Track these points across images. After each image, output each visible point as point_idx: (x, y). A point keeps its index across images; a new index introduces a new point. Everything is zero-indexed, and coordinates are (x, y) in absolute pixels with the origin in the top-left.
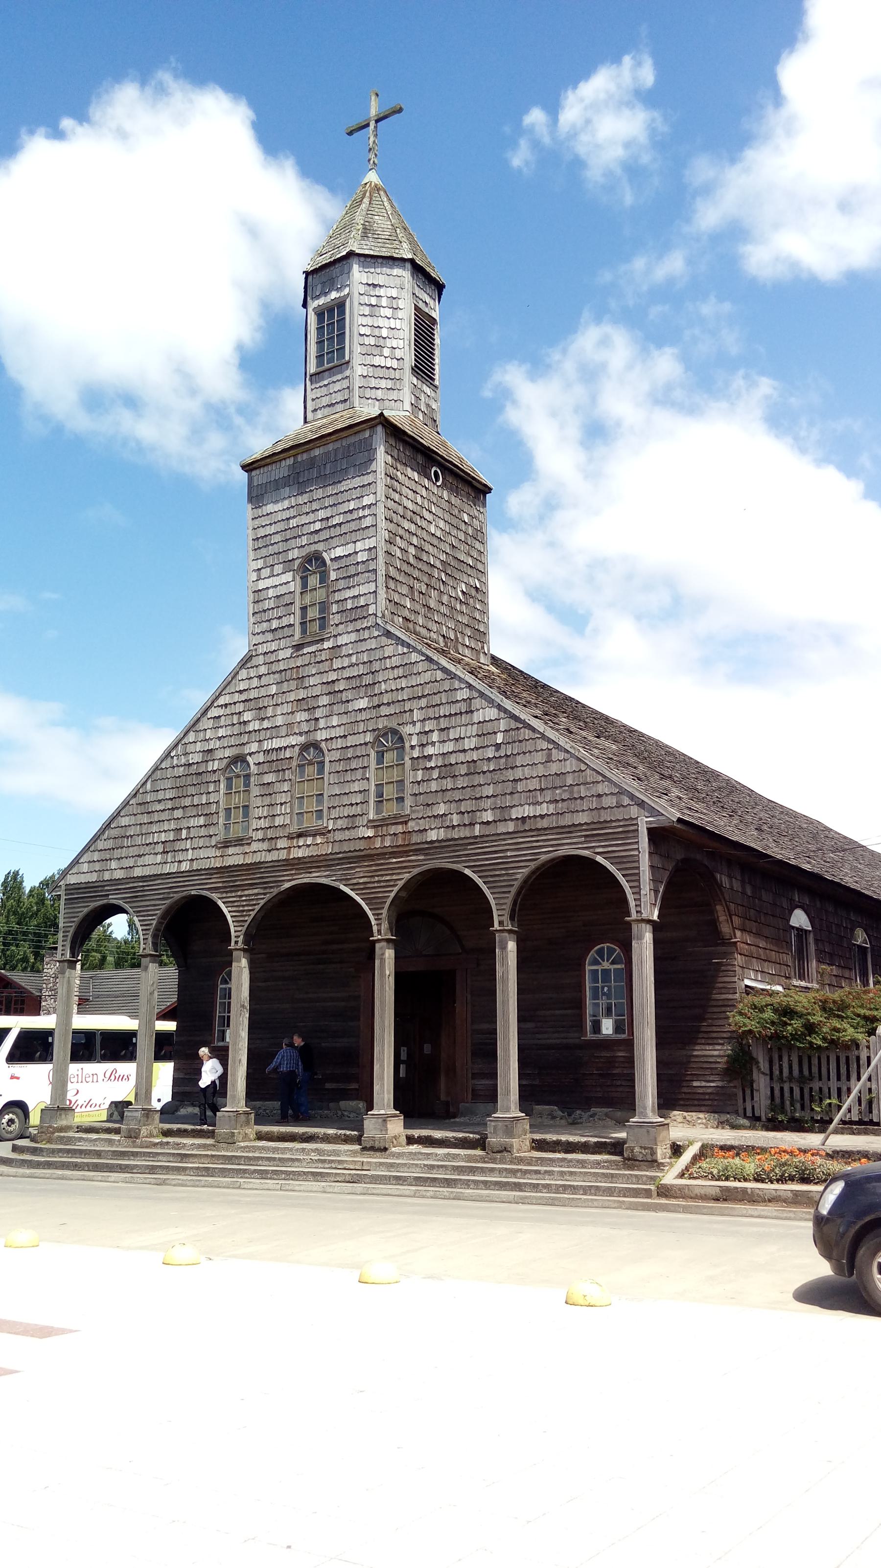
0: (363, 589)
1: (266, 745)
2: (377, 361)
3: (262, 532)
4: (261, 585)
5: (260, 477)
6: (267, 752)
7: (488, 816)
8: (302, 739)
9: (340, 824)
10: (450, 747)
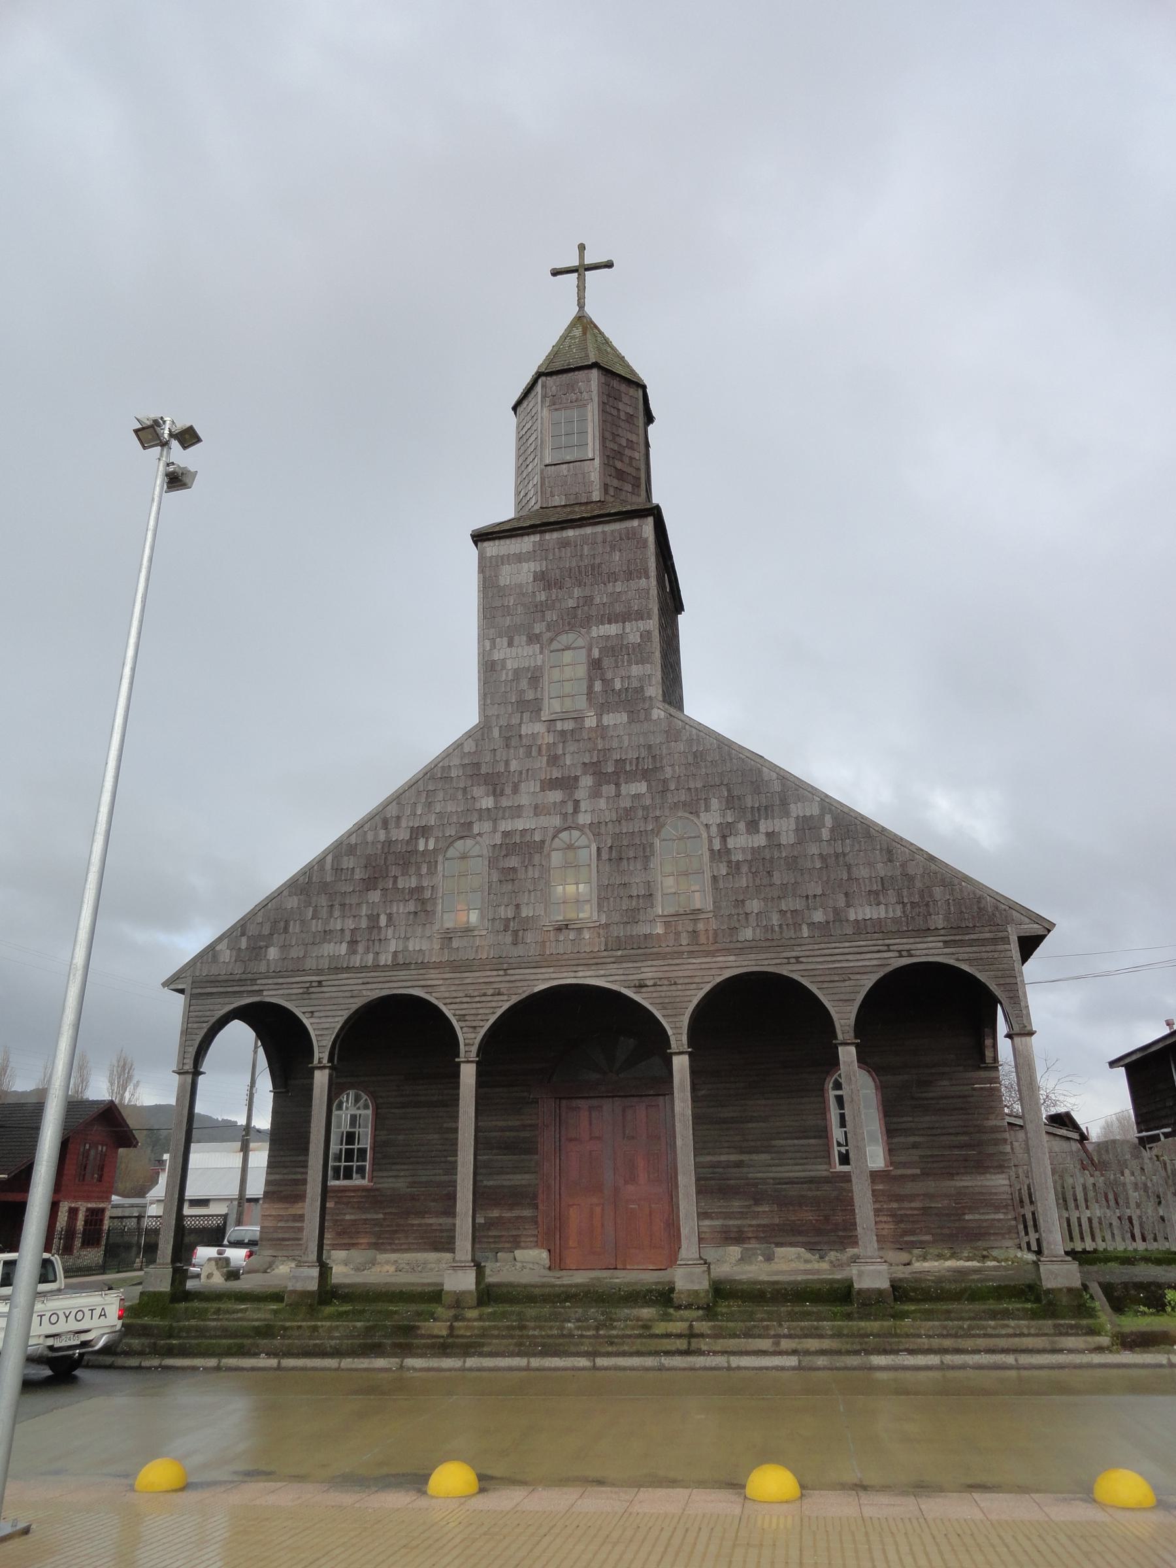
0: (636, 670)
1: (505, 825)
2: (619, 465)
3: (497, 603)
4: (496, 656)
5: (493, 548)
6: (506, 834)
7: (818, 916)
8: (556, 821)
9: (616, 917)
10: (760, 840)
